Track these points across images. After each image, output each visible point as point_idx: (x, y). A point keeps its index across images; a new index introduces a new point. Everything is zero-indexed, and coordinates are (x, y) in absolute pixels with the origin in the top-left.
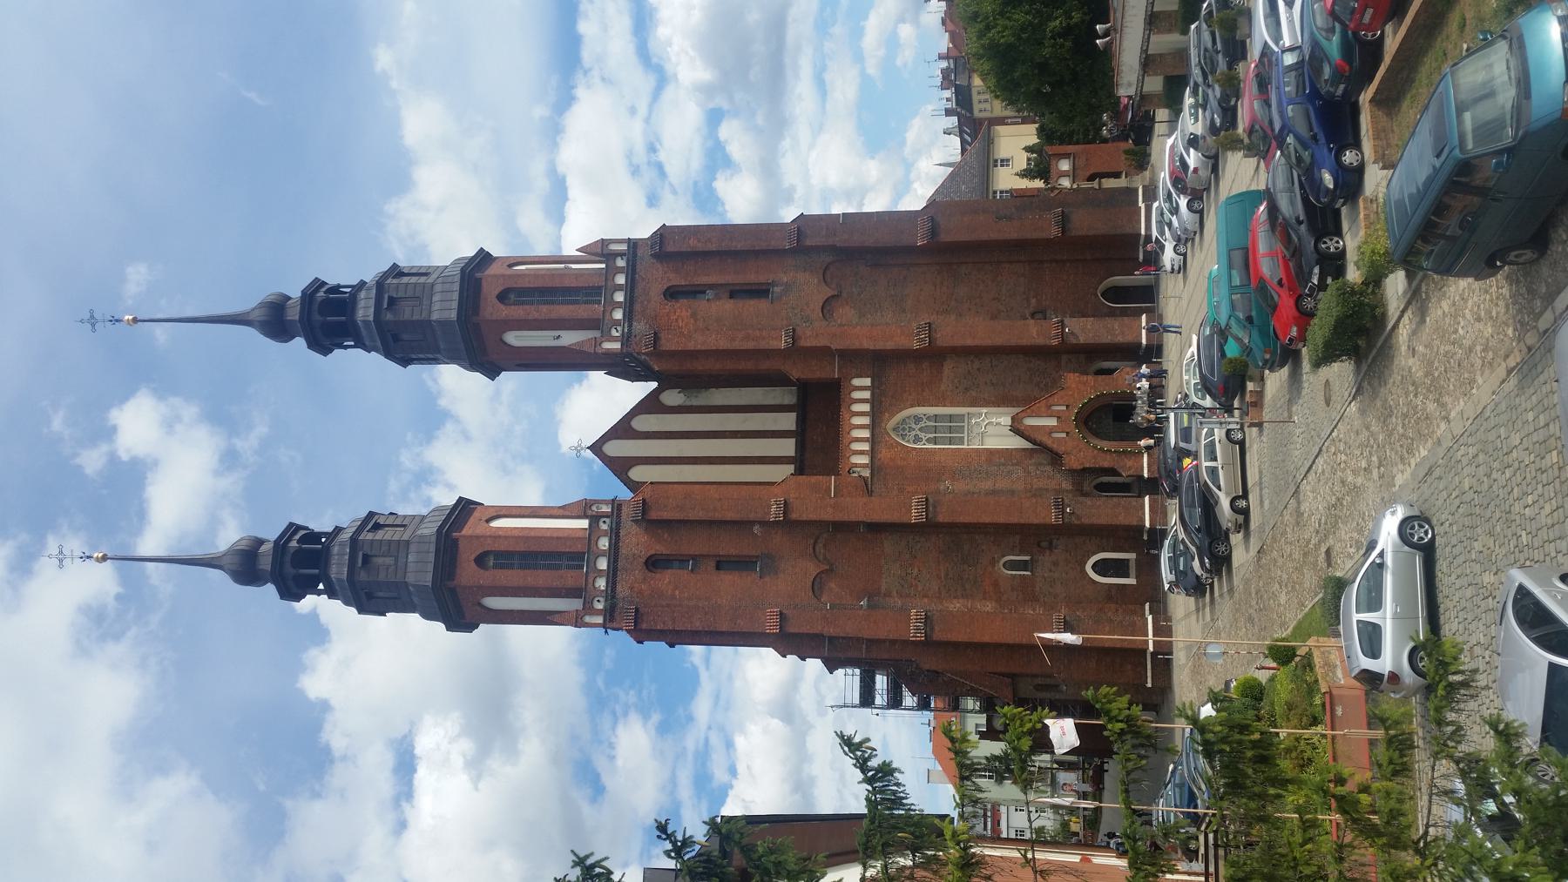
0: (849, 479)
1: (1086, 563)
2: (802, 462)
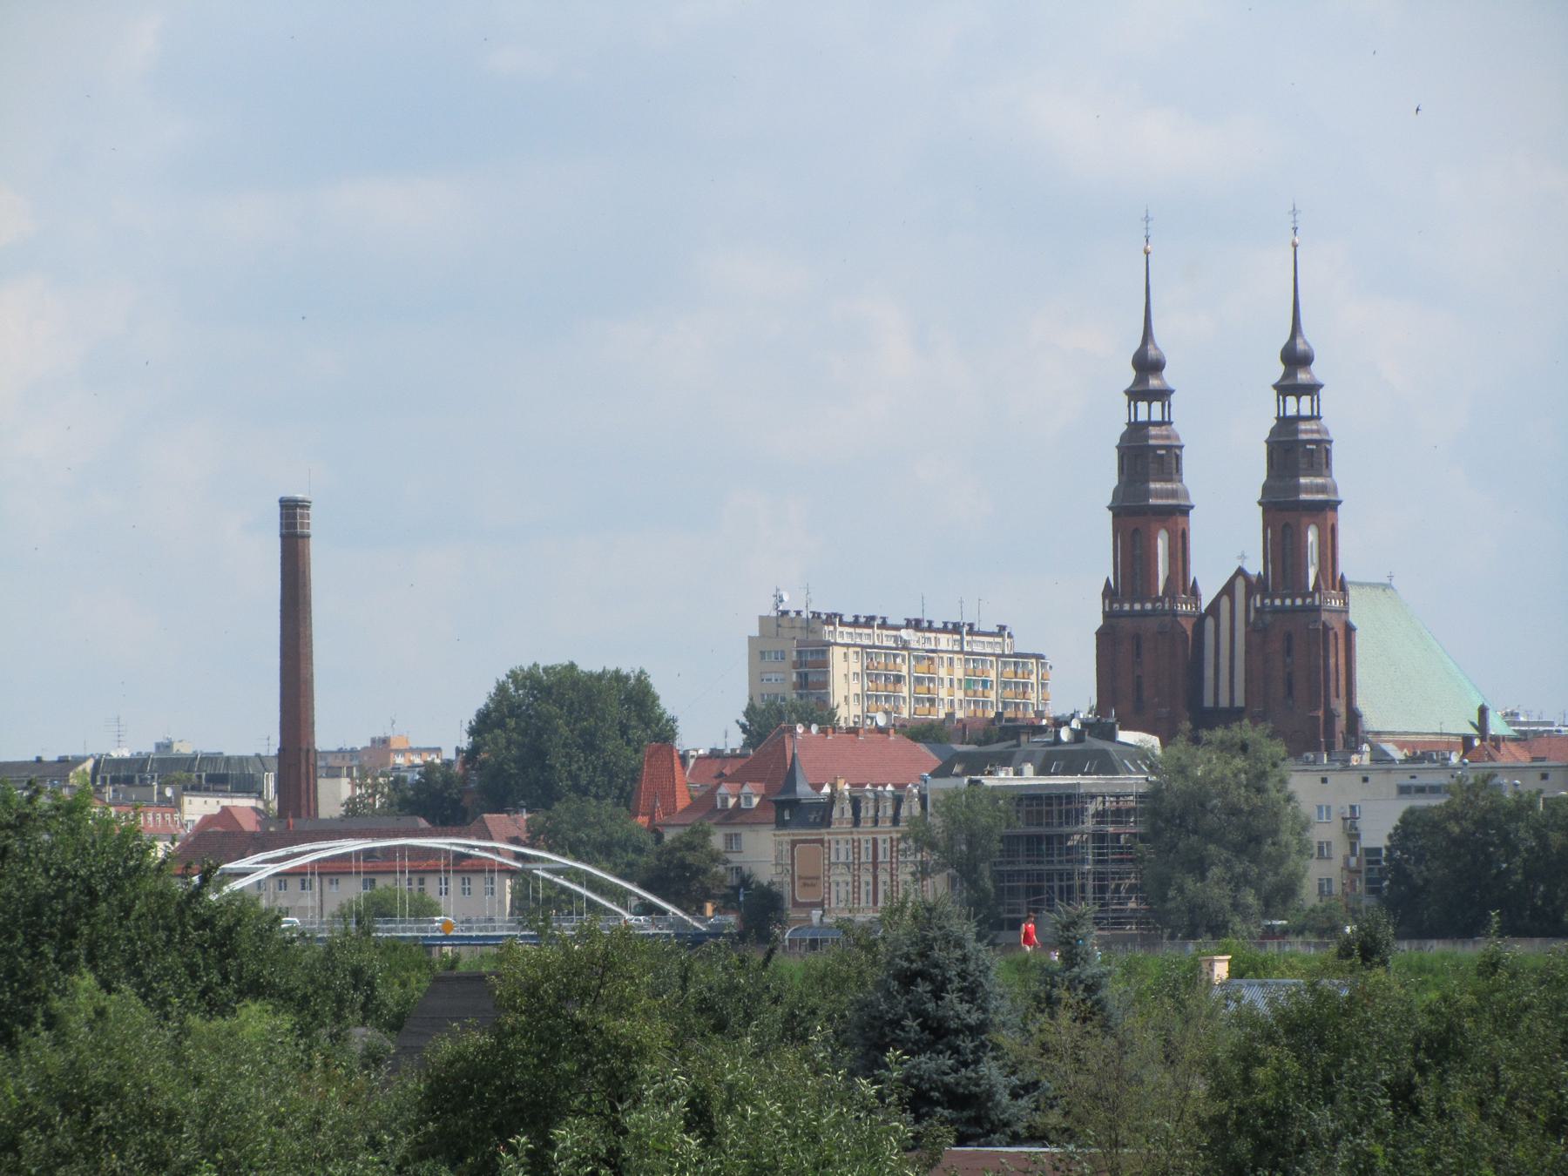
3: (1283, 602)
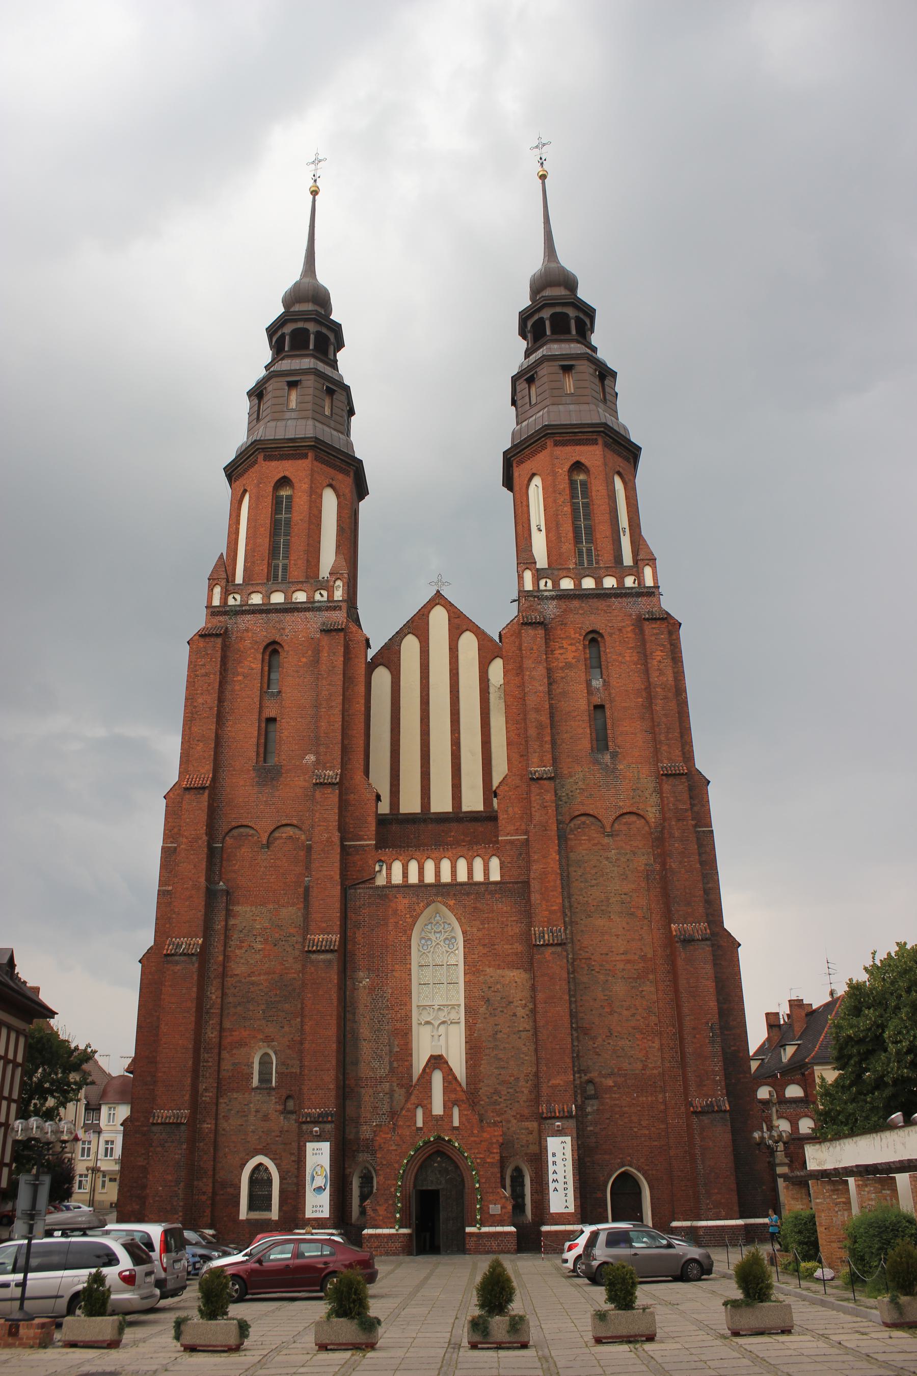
0: (371, 862)
1: (266, 1155)
2: (425, 821)
3: (578, 584)
